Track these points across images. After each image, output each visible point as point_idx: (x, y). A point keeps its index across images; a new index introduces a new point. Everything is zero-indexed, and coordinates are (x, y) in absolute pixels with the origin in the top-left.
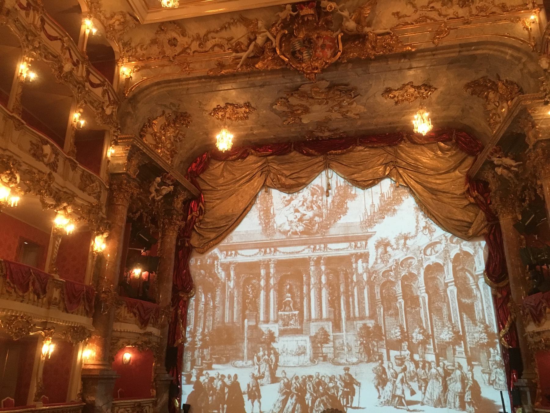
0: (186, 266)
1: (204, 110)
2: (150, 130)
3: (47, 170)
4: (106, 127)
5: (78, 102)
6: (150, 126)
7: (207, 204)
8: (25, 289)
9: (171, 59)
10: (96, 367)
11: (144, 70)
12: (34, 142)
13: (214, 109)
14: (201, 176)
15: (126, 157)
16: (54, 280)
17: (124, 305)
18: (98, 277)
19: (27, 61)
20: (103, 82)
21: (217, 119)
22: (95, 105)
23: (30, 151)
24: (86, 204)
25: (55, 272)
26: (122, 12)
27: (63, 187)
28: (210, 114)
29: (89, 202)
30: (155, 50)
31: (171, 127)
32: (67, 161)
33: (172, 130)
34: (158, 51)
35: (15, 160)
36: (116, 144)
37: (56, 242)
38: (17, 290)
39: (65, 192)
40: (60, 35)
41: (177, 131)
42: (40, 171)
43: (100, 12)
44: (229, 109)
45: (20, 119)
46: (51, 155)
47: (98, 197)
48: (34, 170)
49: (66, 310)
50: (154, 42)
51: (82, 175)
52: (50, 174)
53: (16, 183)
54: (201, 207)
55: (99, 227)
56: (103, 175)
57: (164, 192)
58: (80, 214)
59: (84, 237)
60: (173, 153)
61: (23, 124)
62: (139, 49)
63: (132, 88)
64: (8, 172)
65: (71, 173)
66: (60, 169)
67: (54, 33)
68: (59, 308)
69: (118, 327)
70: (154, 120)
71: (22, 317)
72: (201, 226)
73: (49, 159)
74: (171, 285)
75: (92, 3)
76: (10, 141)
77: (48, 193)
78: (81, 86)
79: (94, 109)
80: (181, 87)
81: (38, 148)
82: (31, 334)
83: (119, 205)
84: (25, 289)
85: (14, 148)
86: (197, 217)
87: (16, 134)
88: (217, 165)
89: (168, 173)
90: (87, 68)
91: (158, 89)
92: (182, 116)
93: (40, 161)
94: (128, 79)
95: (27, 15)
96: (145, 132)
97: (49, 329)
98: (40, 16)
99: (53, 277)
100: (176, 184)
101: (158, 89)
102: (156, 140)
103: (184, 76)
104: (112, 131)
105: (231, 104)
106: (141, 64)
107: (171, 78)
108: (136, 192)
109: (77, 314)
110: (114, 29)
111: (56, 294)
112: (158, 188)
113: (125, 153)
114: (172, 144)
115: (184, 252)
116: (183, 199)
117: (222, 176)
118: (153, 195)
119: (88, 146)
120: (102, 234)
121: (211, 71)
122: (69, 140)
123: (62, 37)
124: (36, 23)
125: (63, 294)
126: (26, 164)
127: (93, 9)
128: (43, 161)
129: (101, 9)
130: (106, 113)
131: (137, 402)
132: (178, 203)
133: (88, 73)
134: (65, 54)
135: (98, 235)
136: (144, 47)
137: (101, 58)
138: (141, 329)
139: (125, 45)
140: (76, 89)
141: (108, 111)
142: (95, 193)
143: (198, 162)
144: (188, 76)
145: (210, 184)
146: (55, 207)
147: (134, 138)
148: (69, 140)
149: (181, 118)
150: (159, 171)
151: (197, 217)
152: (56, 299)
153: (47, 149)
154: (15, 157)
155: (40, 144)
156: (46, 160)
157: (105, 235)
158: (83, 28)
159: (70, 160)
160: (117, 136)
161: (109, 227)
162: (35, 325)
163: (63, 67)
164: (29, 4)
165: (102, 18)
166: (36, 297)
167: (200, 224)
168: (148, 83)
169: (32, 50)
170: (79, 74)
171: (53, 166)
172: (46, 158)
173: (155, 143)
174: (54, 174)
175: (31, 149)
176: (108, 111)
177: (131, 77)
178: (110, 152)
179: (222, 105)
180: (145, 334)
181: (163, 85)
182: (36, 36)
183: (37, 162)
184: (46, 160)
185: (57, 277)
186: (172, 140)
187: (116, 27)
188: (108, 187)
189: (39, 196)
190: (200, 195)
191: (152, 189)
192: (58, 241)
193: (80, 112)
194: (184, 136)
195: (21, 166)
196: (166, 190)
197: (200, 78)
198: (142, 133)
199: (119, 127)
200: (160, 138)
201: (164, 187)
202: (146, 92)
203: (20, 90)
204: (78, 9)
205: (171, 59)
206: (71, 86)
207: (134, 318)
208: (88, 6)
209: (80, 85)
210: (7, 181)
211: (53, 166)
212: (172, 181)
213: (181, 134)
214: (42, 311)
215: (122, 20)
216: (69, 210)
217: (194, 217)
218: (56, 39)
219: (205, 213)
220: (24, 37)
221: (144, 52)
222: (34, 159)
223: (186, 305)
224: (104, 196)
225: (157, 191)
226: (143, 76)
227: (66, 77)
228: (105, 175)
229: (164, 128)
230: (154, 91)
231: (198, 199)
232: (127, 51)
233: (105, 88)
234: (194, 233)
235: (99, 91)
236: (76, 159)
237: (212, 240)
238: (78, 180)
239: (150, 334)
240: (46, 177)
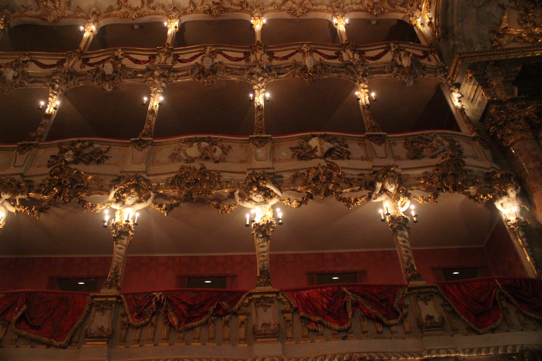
15: (480, 88)
22: (386, 70)
23: (293, 158)
32: (367, 141)
38: (325, 322)
49: (471, 330)
76: (254, 160)
93: (312, 158)
125: (449, 305)
130: (405, 66)
146: (370, 197)
152: (429, 317)
156: (318, 154)
172: (317, 151)
175: (294, 154)
178: (455, 100)
183: (309, 161)
202: (449, 10)
210: (262, 200)
228: (466, 126)
232: (412, 5)
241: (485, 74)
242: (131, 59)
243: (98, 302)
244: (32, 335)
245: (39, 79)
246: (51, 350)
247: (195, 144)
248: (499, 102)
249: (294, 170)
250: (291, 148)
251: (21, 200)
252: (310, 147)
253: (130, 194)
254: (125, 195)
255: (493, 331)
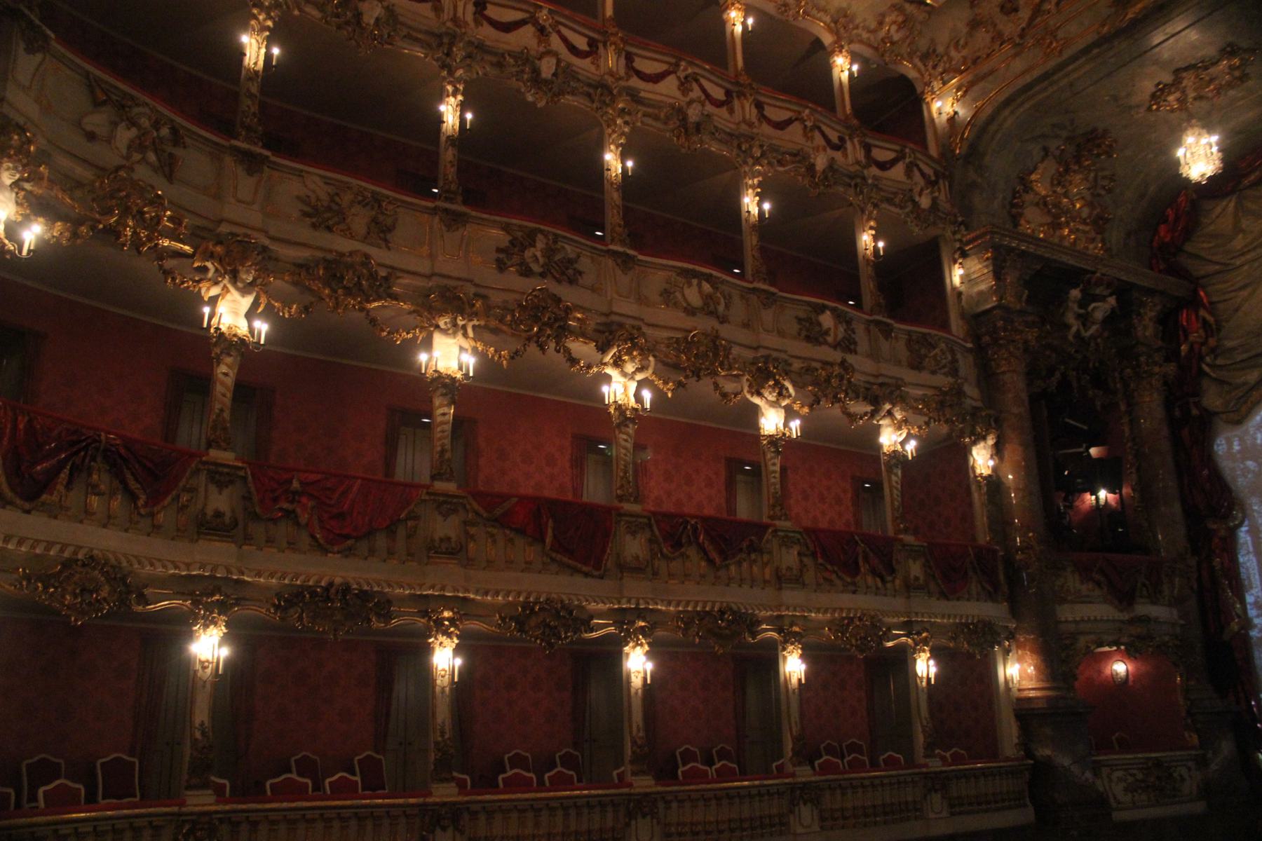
0: (1209, 459)
1: (1130, 107)
2: (1028, 197)
3: (837, 356)
4: (933, 232)
5: (863, 211)
6: (1027, 188)
7: (1221, 306)
8: (853, 570)
9: (1018, 40)
10: (1038, 694)
11: (975, 88)
12: (802, 315)
13: (1153, 96)
14: (1188, 247)
15: (991, 275)
16: (904, 545)
17: (1069, 570)
18: (1000, 522)
19: (753, 187)
20: (902, 151)
21: (1172, 111)
22: (897, 201)
24: (930, 392)
25: (906, 531)
26: (893, 6)
27: (876, 377)
28: (1149, 109)
29: (935, 388)
30: (982, 37)
31: (1075, 171)
32: (872, 327)
33: (1078, 177)
34: (988, 38)
35: (776, 359)
36: (964, 255)
37: (894, 478)
39: (881, 385)
40: (794, 111)
41: (1092, 175)
42: (825, 364)
43: (857, 27)
44: (1189, 81)
45: (765, 287)
46: (836, 327)
47: (954, 372)
48: (814, 364)
49: (944, 596)
50: (974, 25)
51: (909, 342)
52: (843, 363)
53: (790, 396)
54: (1204, 319)
55: (973, 427)
56: (957, 325)
57: (1099, 315)
58: (926, 415)
59: (945, 457)
60: (1100, 223)
61: (774, 294)
62: (953, 53)
63: (963, 133)
64: (771, 383)
65: (885, 345)
66: (863, 346)
67: (783, 115)
68: (930, 594)
69: (1068, 613)
70: (1031, 173)
71: (860, 619)
72: (1219, 362)
73: (836, 335)
74: (1177, 508)
75: (836, 23)
77: (851, 394)
78: (859, 180)
79: (897, 210)
80: (1055, 88)
81: (811, 323)
82: (890, 644)
83: (1004, 373)
84: (853, 570)
85: (771, 341)
86: (1202, 344)
87: (767, 316)
88: (1219, 210)
89: (1094, 273)
90: (860, 142)
91: (1012, 112)
92: (1088, 140)
93: (820, 344)
94: (952, 119)
95: (731, 111)
96: (1021, 207)
97: (919, 633)
98: (751, 99)
99: (901, 540)
100: (1123, 291)
101: (1012, 112)
102: (1049, 211)
103: (1052, 64)
104: (948, 234)
105: (1186, 69)
106: (968, 77)
107: (1028, 79)
108: (1031, 335)
109: (968, 600)
110: (893, 43)
111: (916, 569)
112: (1082, 311)
113: (986, 267)
114: (1091, 205)
115: (1192, 432)
116: (1153, 314)
117: (1238, 229)
118: (1074, 329)
119: (909, 281)
120: (984, 438)
121: (1103, 25)
122: (868, 286)
123: (799, 113)
124: (748, 116)
126: (799, 358)
127: (842, 30)
128: (826, 343)
129: (857, 21)
131: (1148, 759)
132: (1145, 327)
133: (868, 148)
134: (812, 139)
135: (974, 443)
136: (962, 42)
137: (889, 104)
138: (1121, 611)
139: (925, 57)
140: (851, 191)
141: (925, 202)
142: (944, 367)
143: (1171, 218)
144: (1060, 60)
145: (1214, 258)
146: (873, 414)
147: (992, 233)
148: (868, 286)
149: (1087, 146)
150: (1072, 276)
151: (1202, 344)
152: (917, 579)
153: (827, 320)
154: (775, 354)
155: (813, 316)
156: (830, 339)
157: (991, 441)
158: (836, 72)
159: (878, 323)
160: (960, 241)
161: (996, 421)
162: (889, 629)
163: (813, 165)
164: (728, 93)
165: (865, 35)
166: (878, 580)
167: (1216, 358)
168: (988, 111)
169: (754, 165)
170: (851, 159)
171: (848, 345)
173: (1049, 220)
174: (851, 359)
176: (925, 202)
177: (956, 113)
178: (956, 275)
179: (1167, 78)
180: (1132, 621)
181: (1019, 100)
182: (753, 139)
183: (818, 348)
184: (830, 339)
185: (909, 539)
186: (1089, 198)
187: (896, 38)
188: (969, 345)
189: (837, 405)
190: (1195, 292)
191: (1070, 319)
192: (896, 475)
193: (871, 228)
194: (1112, 178)
195: (790, 365)
196: (1100, 310)
197: (1086, 51)
198: (1014, 211)
199: (960, 219)
200: (1057, 205)
201: (1093, 305)
202: (993, 128)
203: (755, 240)
204: (818, 43)
205: (1018, 40)
206: (841, 189)
207: (1097, 592)
208: (830, 30)
209: (856, 180)
211: (848, 345)
212: (1109, 285)
213: (1104, 178)
214: (899, 603)
215: (900, 19)
216: (898, 416)
217: (1196, 347)
218: (788, 122)
219: (1219, 330)
220: (735, 151)
221: (965, 52)
222: (810, 345)
223: (1230, 546)
224: (966, 365)
225: (1079, 316)
226: (975, 100)
227: (826, 178)
228: (961, 322)
229: (1059, 180)
230: (1005, 120)
231: (1193, 302)
232: (934, 67)
233: (907, 160)
234: (1205, 383)
235: (898, 172)
236: (889, 317)
237: (1252, 389)
238: (903, 353)
239: (1145, 620)
240: (837, 370)
241: (1005, 261)
242: (565, 40)
243: (627, 522)
244: (565, 560)
245: (414, 34)
246: (589, 580)
247: (695, 282)
248: (1006, 309)
249: (805, 359)
250: (799, 320)
251: (474, 327)
252: (820, 324)
253: (633, 359)
254: (626, 358)
255: (958, 599)
